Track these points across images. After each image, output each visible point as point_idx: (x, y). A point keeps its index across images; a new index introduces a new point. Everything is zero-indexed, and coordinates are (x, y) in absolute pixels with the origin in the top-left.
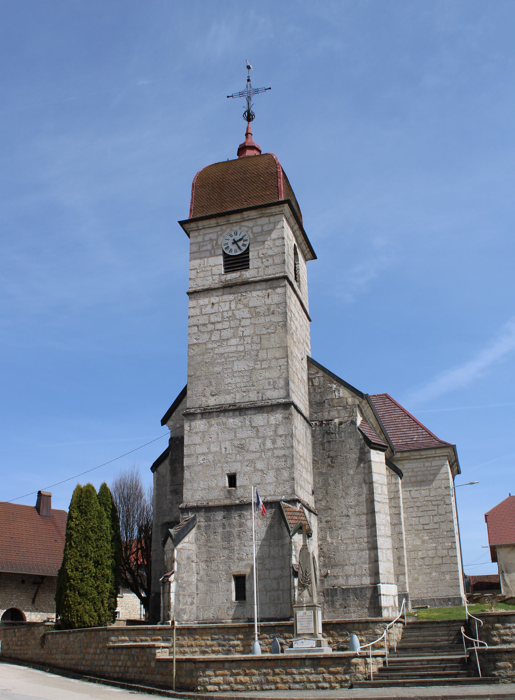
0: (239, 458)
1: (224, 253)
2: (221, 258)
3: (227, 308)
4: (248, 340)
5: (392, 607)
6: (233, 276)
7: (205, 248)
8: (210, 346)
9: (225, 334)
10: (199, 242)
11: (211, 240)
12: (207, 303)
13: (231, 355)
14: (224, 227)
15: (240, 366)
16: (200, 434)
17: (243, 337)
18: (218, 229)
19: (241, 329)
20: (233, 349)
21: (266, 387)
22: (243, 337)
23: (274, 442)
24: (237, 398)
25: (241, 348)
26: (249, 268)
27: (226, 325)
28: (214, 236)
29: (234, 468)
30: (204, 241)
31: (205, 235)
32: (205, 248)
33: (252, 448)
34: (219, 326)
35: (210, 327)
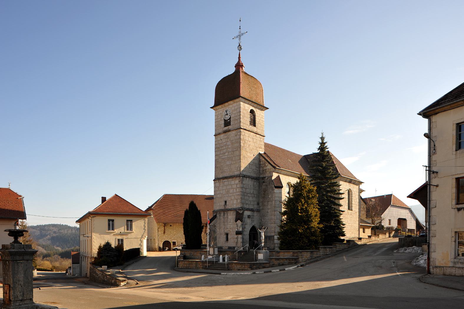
0: (227, 195)
2: (223, 121)
3: (225, 141)
4: (230, 153)
6: (226, 128)
7: (219, 117)
8: (220, 156)
9: (224, 151)
10: (217, 115)
11: (220, 113)
12: (219, 139)
13: (226, 159)
14: (224, 108)
15: (228, 163)
16: (218, 187)
17: (229, 152)
18: (223, 108)
19: (229, 149)
20: (226, 157)
21: (235, 171)
23: (236, 190)
24: (227, 174)
26: (230, 125)
28: (221, 112)
29: (225, 199)
30: (219, 114)
31: (219, 111)
32: (219, 117)
33: (231, 192)
34: (223, 148)
35: (220, 148)
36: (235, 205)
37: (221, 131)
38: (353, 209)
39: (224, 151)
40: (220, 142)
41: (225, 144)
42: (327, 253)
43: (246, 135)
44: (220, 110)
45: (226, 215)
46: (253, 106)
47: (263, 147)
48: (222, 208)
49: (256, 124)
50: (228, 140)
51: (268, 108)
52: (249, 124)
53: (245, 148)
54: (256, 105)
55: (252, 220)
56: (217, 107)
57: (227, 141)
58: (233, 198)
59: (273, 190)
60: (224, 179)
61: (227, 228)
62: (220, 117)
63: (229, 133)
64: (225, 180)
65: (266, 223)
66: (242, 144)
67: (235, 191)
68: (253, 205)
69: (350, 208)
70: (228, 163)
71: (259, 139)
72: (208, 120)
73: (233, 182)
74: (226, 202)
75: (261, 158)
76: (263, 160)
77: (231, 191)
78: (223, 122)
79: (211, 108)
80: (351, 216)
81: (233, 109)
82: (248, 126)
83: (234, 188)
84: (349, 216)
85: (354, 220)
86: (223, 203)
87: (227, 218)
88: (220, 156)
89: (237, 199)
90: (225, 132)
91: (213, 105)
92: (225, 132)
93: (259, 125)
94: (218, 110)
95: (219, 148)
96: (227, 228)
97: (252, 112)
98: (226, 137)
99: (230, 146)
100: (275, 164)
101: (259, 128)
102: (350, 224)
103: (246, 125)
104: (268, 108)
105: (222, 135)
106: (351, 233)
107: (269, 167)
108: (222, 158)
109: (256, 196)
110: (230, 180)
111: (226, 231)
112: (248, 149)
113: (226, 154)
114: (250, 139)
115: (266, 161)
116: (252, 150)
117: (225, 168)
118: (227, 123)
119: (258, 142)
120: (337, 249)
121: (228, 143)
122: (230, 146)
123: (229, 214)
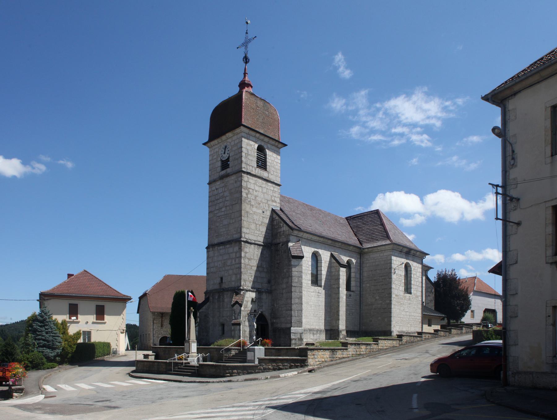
0: (224, 269)
1: (221, 160)
4: (228, 208)
5: (299, 339)
6: (224, 172)
8: (216, 212)
9: (221, 205)
14: (221, 144)
17: (226, 207)
18: (219, 145)
20: (223, 213)
22: (226, 207)
23: (235, 261)
25: (226, 213)
27: (221, 200)
28: (217, 150)
34: (219, 202)
35: (216, 201)
36: (233, 283)
37: (216, 176)
38: (412, 292)
39: (221, 205)
40: (216, 192)
41: (222, 194)
42: (362, 353)
43: (251, 181)
44: (216, 146)
45: (222, 297)
46: (262, 140)
47: (278, 200)
48: (217, 287)
49: (268, 167)
50: (226, 189)
51: (286, 145)
52: (256, 166)
53: (249, 200)
54: (266, 139)
55: (258, 305)
56: (212, 143)
57: (225, 191)
58: (231, 272)
59: (290, 261)
60: (220, 246)
61: (223, 317)
62: (215, 157)
63: (226, 180)
64: (221, 247)
65: (280, 309)
66: (244, 195)
67: (233, 261)
68: (262, 283)
69: (408, 290)
70: (225, 222)
71: (272, 188)
72: (199, 162)
73: (231, 250)
74: (222, 278)
75: (275, 216)
76: (277, 218)
77: (229, 262)
78: (219, 164)
79: (204, 144)
80: (409, 302)
81: (233, 143)
82: (254, 169)
83: (232, 259)
84: (406, 301)
85: (414, 308)
86: (218, 280)
87: (223, 301)
88: (216, 212)
89: (236, 274)
90: (222, 178)
91: (207, 140)
92: (222, 178)
93: (273, 169)
94: (214, 147)
95: (214, 201)
96: (223, 317)
97: (261, 149)
98: (223, 185)
99: (228, 198)
100: (293, 223)
101: (272, 173)
102: (408, 313)
103: (251, 167)
104: (286, 145)
105: (218, 183)
106: (409, 325)
107: (285, 228)
108: (218, 215)
109: (265, 270)
110: (228, 246)
111: (221, 321)
112: (253, 203)
113: (223, 209)
114: (257, 188)
115: (280, 220)
116: (259, 204)
117: (221, 230)
118: (225, 164)
119: (271, 193)
120: (380, 347)
121: (226, 194)
122: (228, 198)
123: (225, 296)
